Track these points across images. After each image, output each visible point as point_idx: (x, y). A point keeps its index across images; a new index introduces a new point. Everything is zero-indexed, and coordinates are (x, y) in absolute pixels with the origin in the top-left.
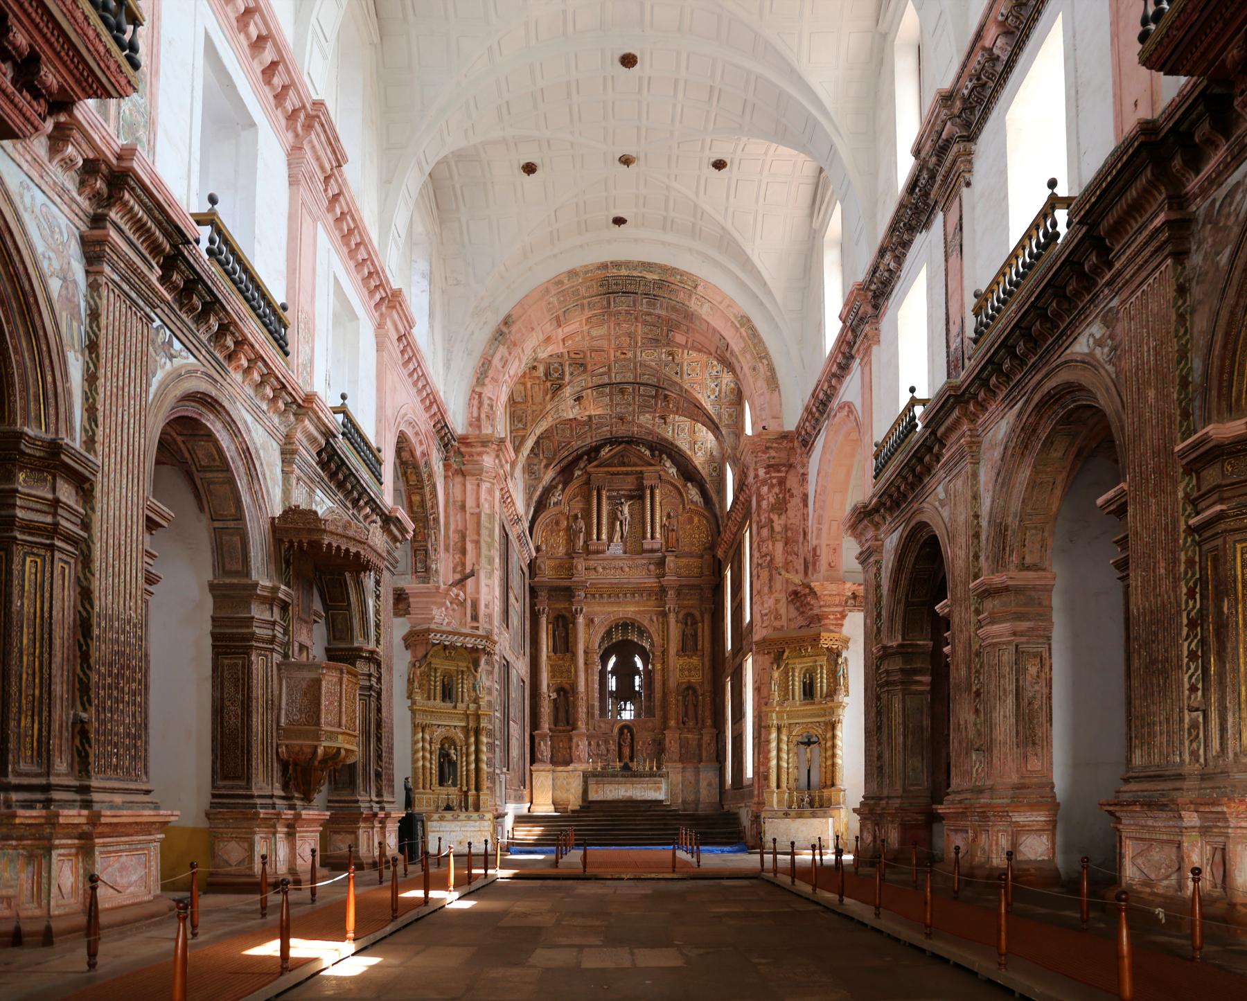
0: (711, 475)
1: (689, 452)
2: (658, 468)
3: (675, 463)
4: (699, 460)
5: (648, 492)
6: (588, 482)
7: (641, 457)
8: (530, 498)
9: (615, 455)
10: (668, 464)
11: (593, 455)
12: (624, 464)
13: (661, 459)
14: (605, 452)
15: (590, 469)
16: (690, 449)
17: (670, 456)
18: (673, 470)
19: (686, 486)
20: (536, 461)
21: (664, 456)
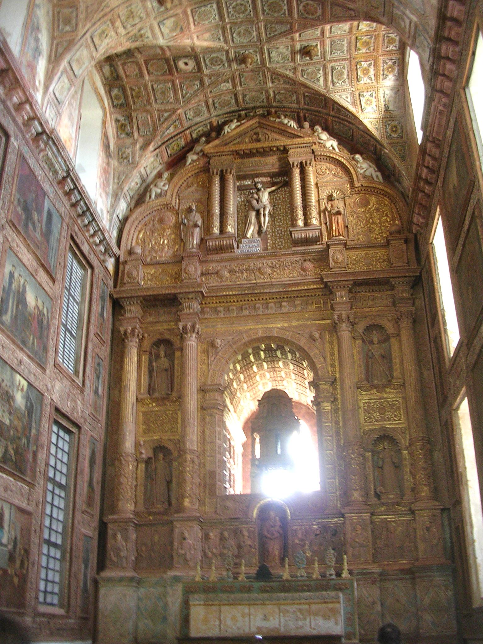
0: (389, 137)
1: (351, 108)
2: (308, 139)
3: (332, 134)
4: (369, 117)
5: (297, 172)
6: (206, 169)
7: (284, 132)
8: (120, 188)
9: (245, 133)
10: (324, 136)
11: (214, 134)
12: (258, 141)
13: (313, 131)
14: (231, 129)
15: (209, 148)
16: (354, 104)
17: (326, 129)
18: (331, 143)
19: (353, 159)
20: (129, 141)
21: (318, 128)
